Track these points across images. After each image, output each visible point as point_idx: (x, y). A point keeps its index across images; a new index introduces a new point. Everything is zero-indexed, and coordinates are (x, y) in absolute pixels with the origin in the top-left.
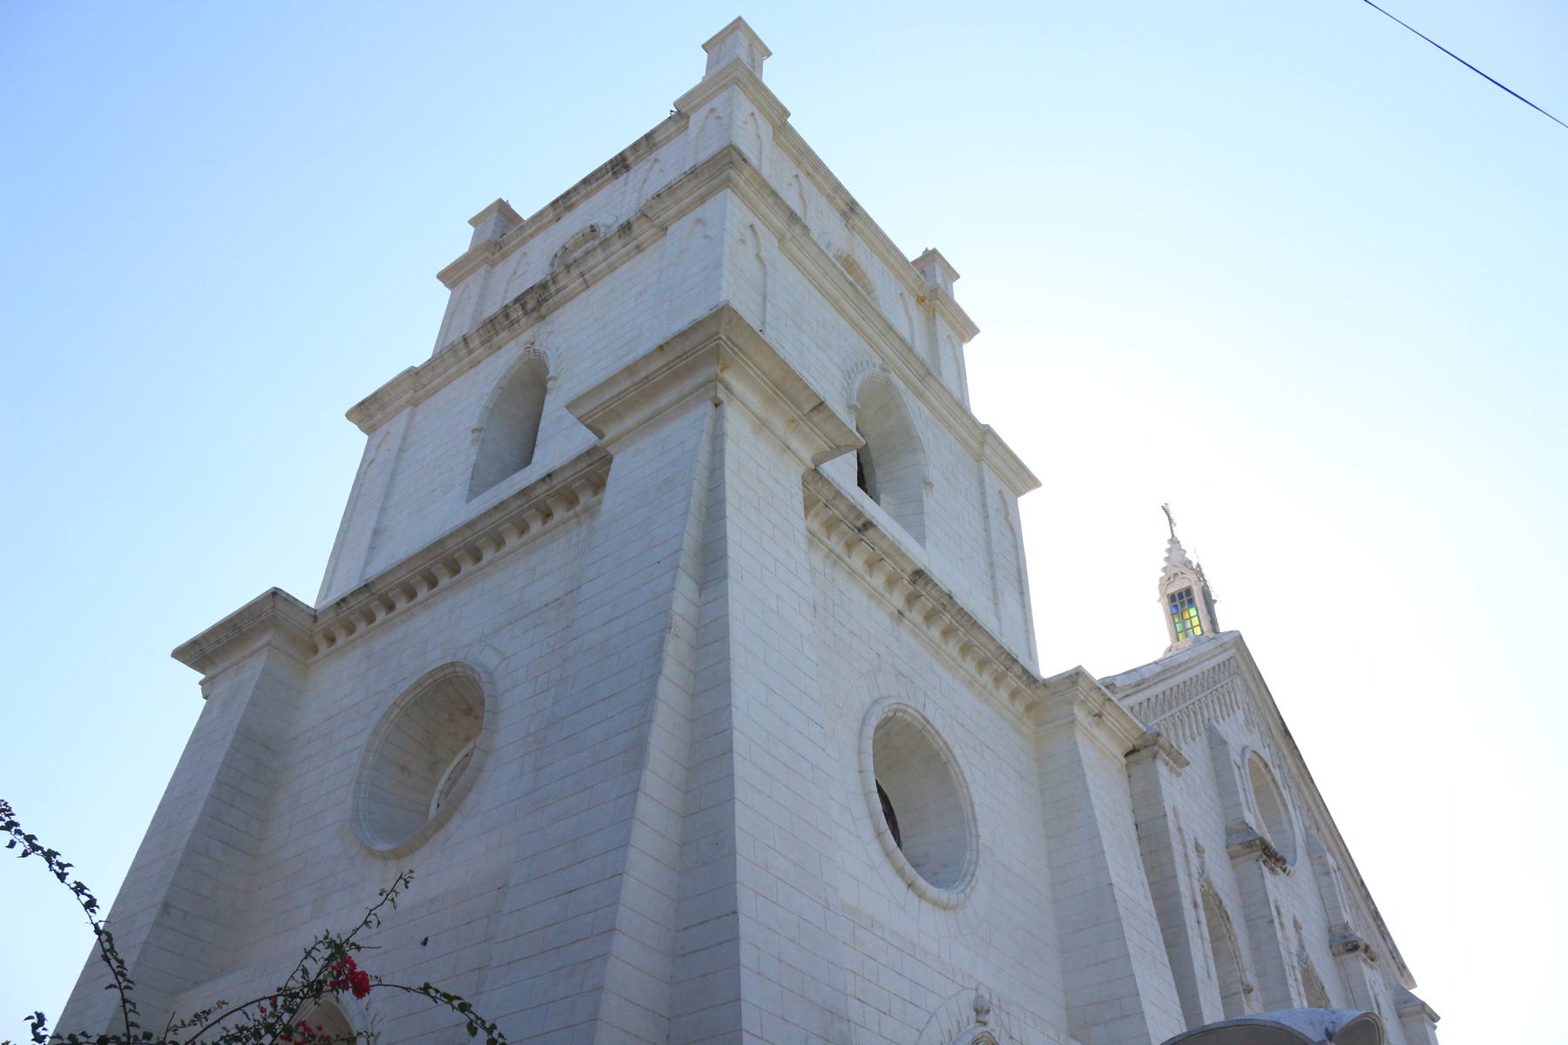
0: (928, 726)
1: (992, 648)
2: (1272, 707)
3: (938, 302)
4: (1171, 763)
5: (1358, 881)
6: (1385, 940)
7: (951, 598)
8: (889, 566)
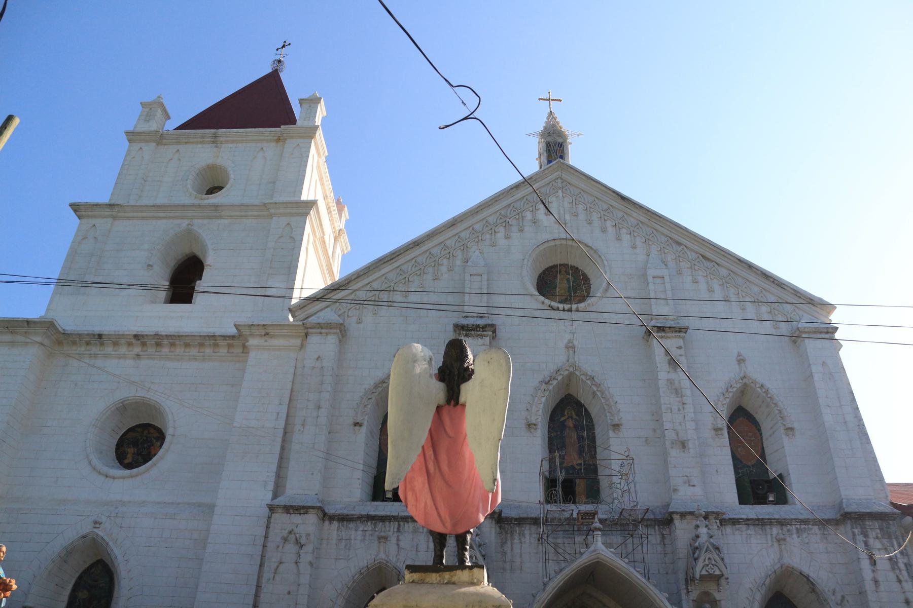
0: (144, 399)
1: (199, 338)
2: (603, 188)
3: (284, 135)
4: (323, 331)
5: (737, 261)
6: (784, 289)
7: (158, 335)
8: (123, 341)
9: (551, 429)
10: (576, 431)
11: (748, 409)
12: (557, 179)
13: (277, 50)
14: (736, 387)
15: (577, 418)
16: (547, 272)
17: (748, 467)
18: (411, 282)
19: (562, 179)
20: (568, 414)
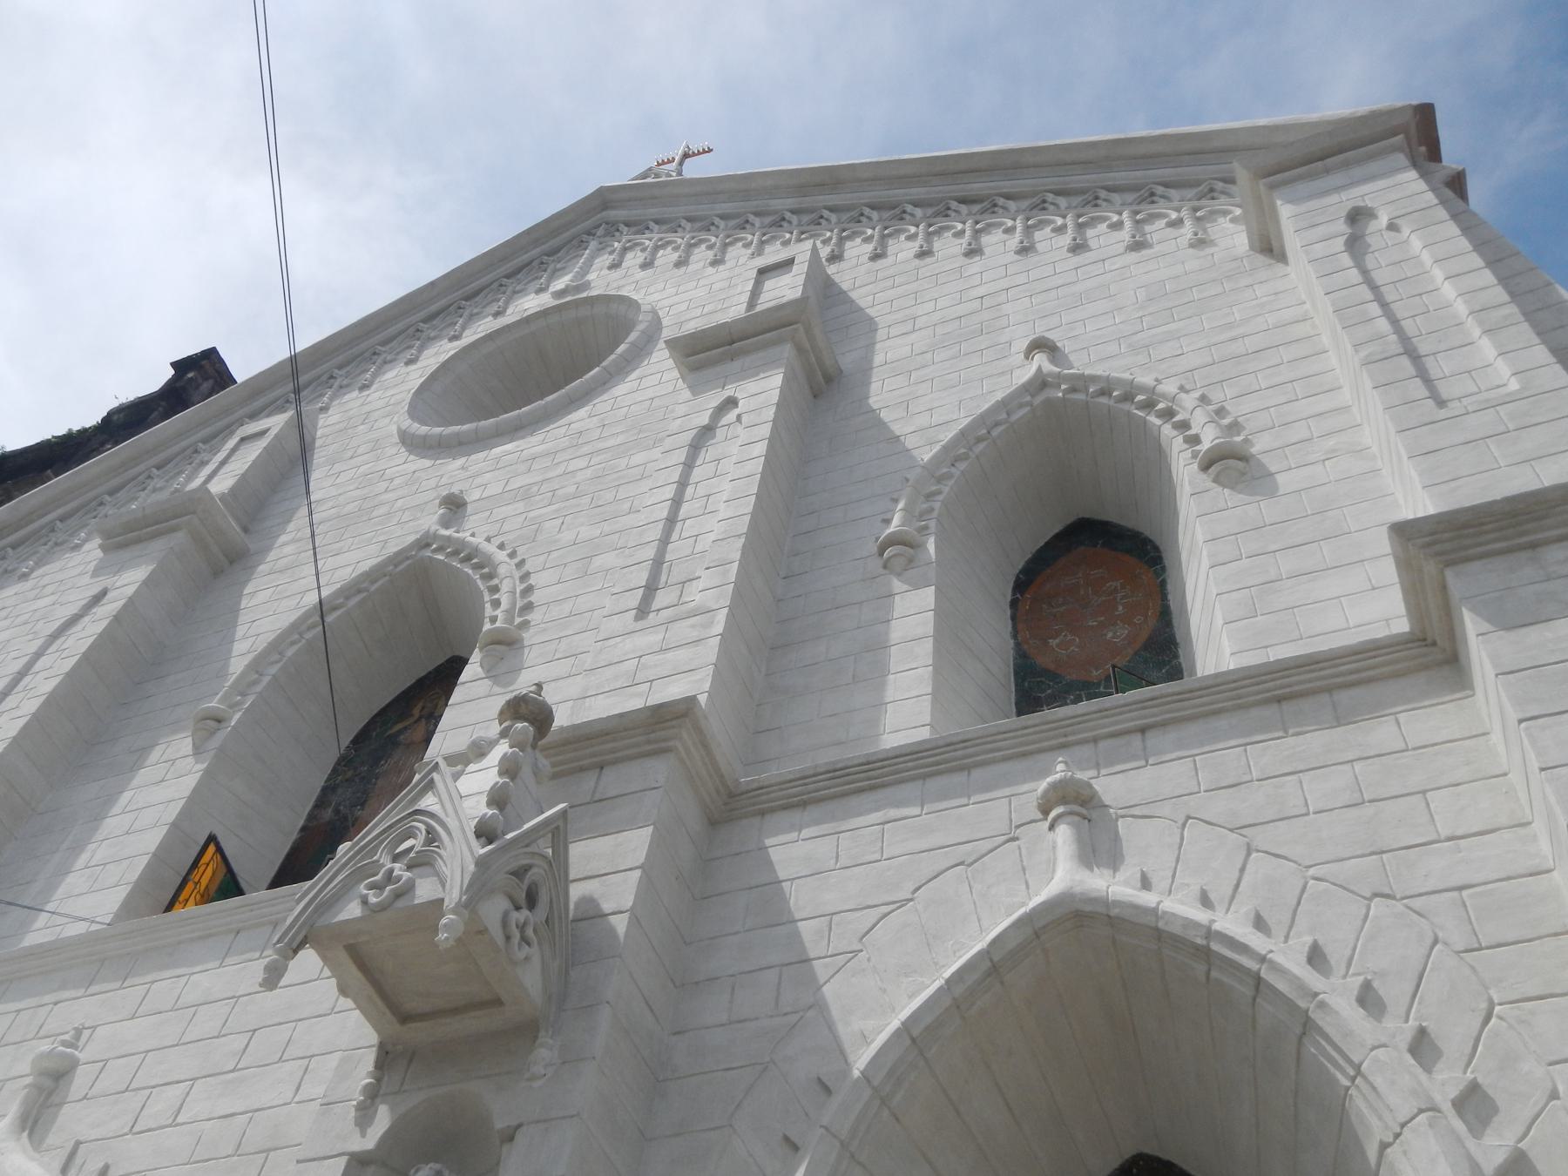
11: (1111, 515)
19: (607, 223)
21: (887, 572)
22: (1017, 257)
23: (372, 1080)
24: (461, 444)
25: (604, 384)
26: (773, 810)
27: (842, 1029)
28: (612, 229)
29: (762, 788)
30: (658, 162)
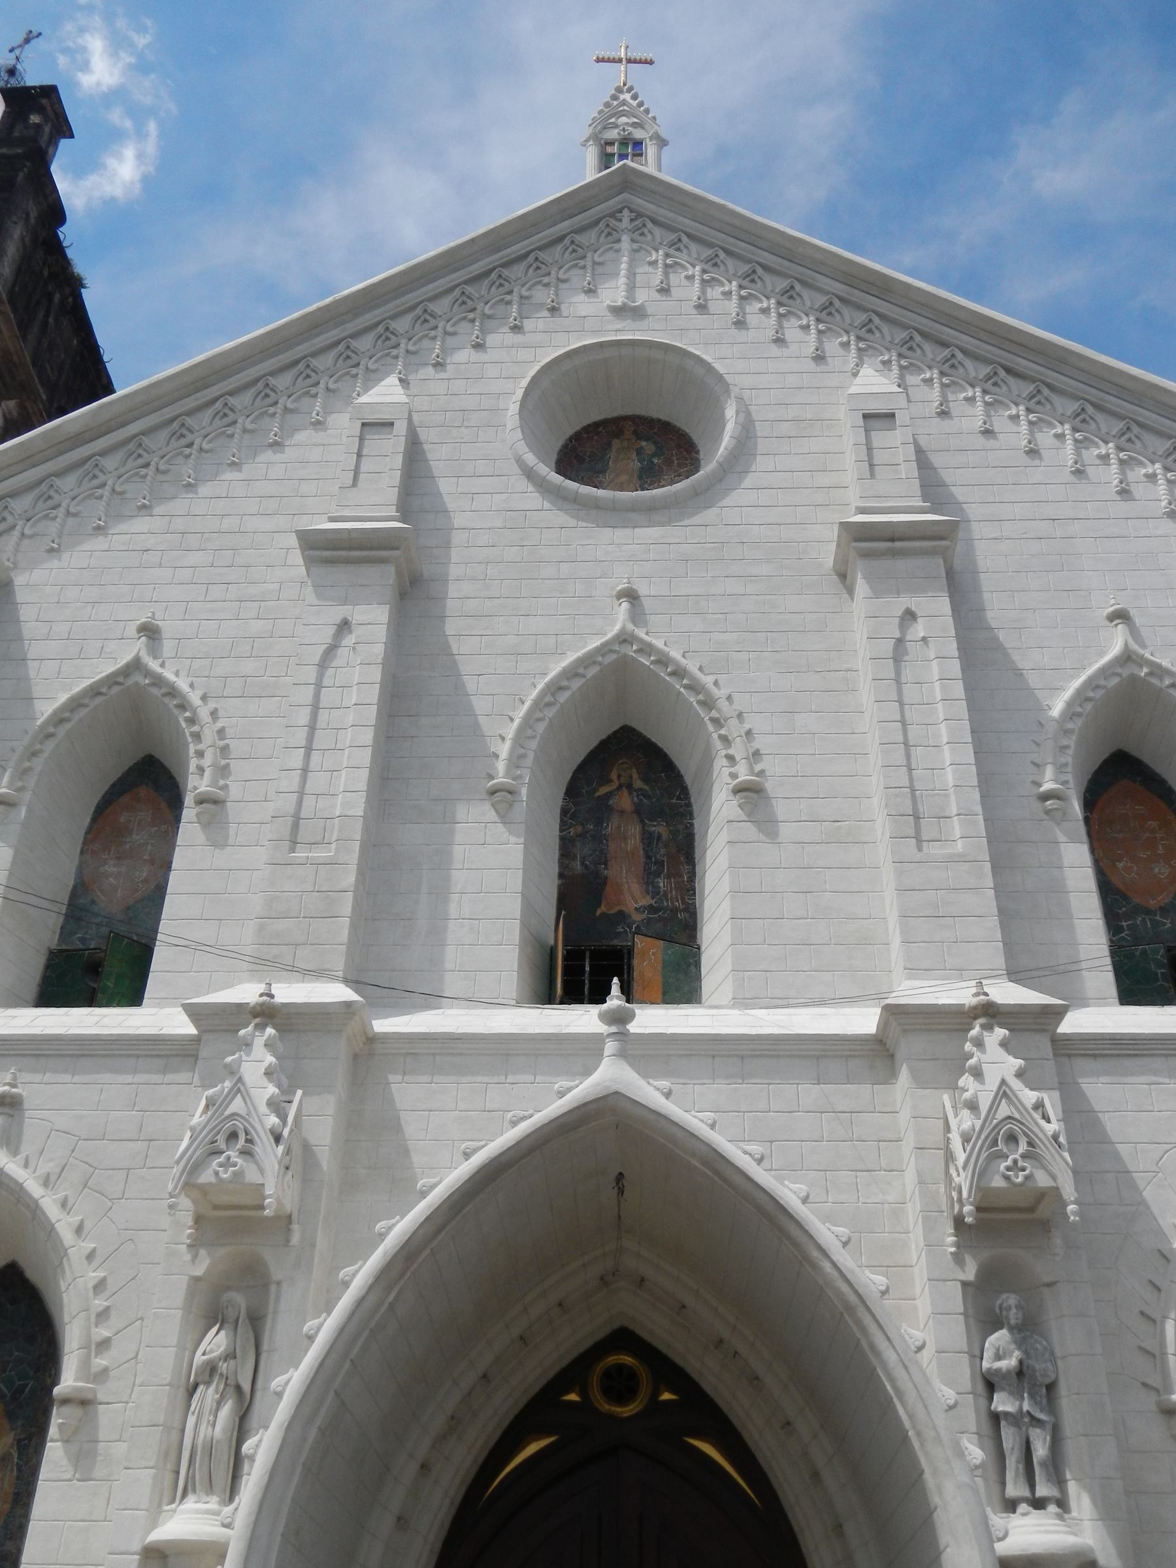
9: (567, 816)
10: (642, 821)
11: (1146, 758)
12: (620, 211)
13: (11, 51)
14: (1104, 687)
15: (646, 787)
16: (585, 436)
17: (1148, 912)
18: (207, 452)
19: (631, 211)
20: (619, 777)
21: (1046, 817)
22: (1072, 478)
23: (955, 1238)
24: (598, 507)
25: (721, 480)
26: (1076, 1055)
27: (1161, 1223)
28: (641, 222)
29: (1069, 1040)
30: (598, 58)
